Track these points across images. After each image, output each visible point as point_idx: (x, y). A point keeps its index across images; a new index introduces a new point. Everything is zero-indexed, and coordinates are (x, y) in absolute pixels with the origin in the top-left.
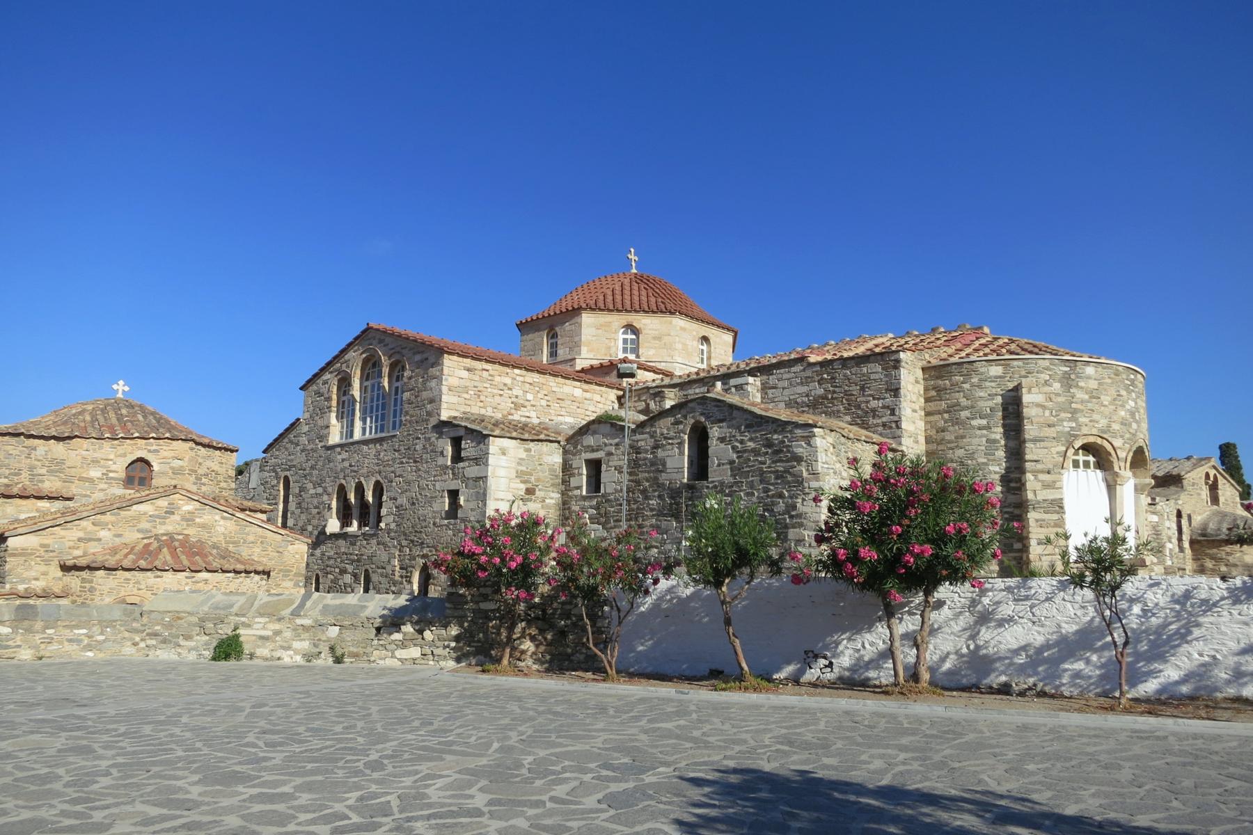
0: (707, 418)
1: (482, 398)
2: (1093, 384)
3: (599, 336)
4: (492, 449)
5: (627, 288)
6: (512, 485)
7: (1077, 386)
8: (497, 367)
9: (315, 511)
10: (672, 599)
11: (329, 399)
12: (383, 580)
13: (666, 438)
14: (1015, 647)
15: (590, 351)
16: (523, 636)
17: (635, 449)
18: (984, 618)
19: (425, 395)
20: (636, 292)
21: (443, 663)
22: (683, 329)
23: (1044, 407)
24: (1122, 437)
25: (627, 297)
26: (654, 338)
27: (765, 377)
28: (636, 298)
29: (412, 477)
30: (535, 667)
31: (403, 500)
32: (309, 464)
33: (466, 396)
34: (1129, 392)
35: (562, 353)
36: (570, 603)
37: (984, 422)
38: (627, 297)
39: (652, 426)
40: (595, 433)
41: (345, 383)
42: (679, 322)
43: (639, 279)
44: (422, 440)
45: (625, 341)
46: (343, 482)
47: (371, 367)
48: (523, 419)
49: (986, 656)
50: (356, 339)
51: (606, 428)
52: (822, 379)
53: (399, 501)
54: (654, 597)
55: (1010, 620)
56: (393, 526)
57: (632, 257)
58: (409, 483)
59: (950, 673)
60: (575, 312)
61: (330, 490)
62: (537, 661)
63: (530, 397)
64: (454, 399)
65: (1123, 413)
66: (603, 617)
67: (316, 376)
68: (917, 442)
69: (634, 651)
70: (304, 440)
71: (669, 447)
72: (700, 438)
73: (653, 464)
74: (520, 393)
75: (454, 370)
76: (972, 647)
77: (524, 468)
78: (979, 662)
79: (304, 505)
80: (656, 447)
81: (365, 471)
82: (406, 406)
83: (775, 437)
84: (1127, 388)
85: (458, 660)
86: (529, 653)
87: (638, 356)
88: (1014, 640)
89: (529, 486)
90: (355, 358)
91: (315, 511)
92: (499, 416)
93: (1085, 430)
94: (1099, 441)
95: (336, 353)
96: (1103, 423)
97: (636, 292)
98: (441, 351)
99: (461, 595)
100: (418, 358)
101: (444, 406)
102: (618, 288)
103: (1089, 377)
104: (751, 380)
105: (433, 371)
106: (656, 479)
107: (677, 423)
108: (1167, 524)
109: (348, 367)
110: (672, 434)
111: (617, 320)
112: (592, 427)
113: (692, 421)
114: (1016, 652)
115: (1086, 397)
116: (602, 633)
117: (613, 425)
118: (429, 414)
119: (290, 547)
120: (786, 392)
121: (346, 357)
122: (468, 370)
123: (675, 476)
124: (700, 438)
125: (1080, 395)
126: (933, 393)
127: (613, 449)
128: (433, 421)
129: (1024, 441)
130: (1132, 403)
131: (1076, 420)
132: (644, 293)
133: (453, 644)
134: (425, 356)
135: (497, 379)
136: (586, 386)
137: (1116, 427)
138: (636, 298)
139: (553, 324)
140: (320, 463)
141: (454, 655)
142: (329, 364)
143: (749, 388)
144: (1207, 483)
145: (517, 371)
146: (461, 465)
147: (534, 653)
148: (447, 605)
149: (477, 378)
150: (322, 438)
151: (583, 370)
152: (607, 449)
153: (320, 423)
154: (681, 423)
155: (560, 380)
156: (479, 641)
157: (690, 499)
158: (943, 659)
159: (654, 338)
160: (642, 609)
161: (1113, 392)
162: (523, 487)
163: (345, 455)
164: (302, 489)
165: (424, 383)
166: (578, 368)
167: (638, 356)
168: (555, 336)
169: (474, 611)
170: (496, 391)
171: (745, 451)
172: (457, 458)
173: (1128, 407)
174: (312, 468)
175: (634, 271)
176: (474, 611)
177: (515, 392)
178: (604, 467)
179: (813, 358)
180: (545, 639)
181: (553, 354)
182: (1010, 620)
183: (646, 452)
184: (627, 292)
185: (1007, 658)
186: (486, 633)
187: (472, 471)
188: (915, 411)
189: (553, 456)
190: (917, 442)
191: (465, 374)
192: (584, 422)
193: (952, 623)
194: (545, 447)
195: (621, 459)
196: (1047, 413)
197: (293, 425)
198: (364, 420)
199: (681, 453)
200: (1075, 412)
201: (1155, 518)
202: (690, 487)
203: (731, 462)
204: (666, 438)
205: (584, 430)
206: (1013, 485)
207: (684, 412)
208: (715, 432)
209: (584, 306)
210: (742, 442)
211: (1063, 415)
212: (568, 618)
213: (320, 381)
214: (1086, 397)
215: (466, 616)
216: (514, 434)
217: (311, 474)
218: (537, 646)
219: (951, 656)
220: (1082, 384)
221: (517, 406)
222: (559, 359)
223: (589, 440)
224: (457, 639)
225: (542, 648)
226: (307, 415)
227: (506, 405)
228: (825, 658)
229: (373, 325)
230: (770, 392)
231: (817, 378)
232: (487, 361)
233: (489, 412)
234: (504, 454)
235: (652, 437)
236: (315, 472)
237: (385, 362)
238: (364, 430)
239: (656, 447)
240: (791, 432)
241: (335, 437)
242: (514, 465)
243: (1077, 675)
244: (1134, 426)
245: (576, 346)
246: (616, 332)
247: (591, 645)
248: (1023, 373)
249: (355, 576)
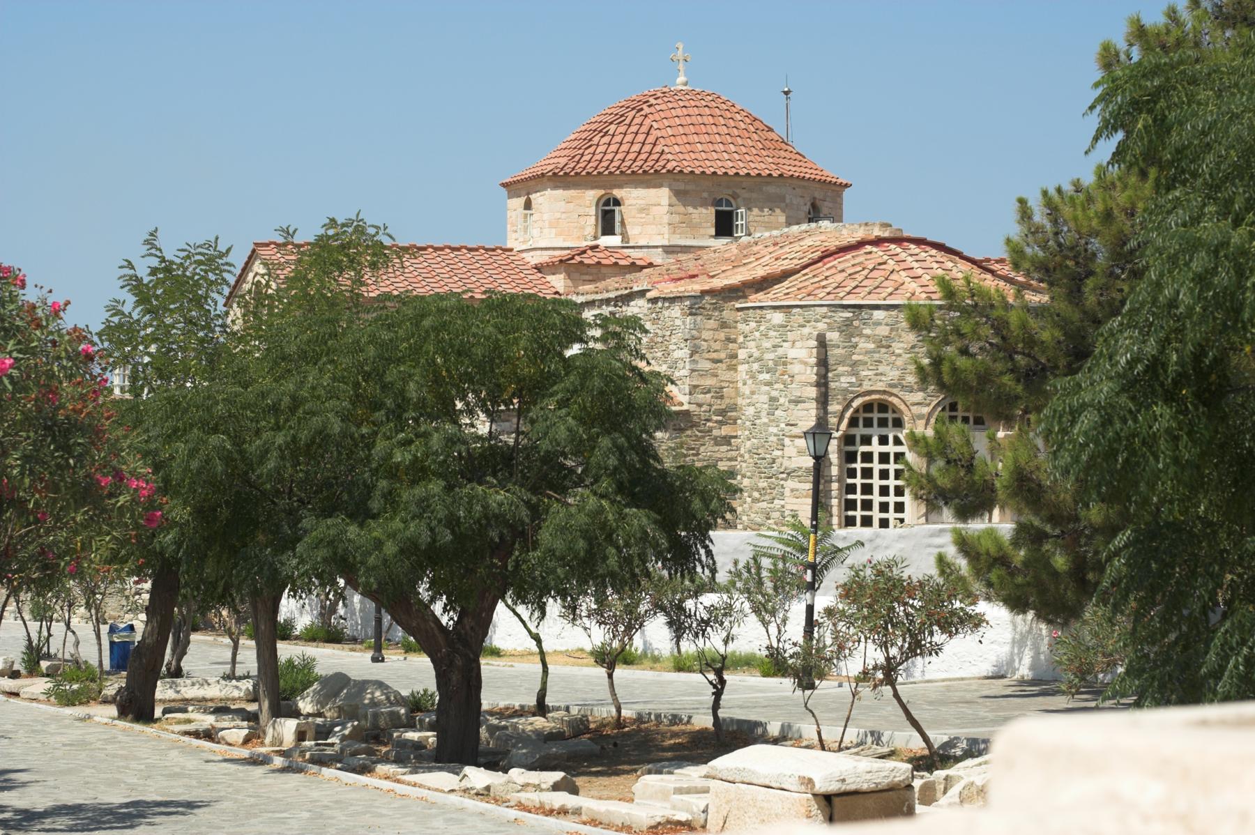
2: (883, 331)
7: (861, 335)
23: (806, 364)
93: (866, 386)
96: (893, 374)
103: (878, 324)
115: (873, 346)
125: (864, 345)
131: (856, 374)
200: (855, 364)
220: (867, 331)
248: (801, 320)
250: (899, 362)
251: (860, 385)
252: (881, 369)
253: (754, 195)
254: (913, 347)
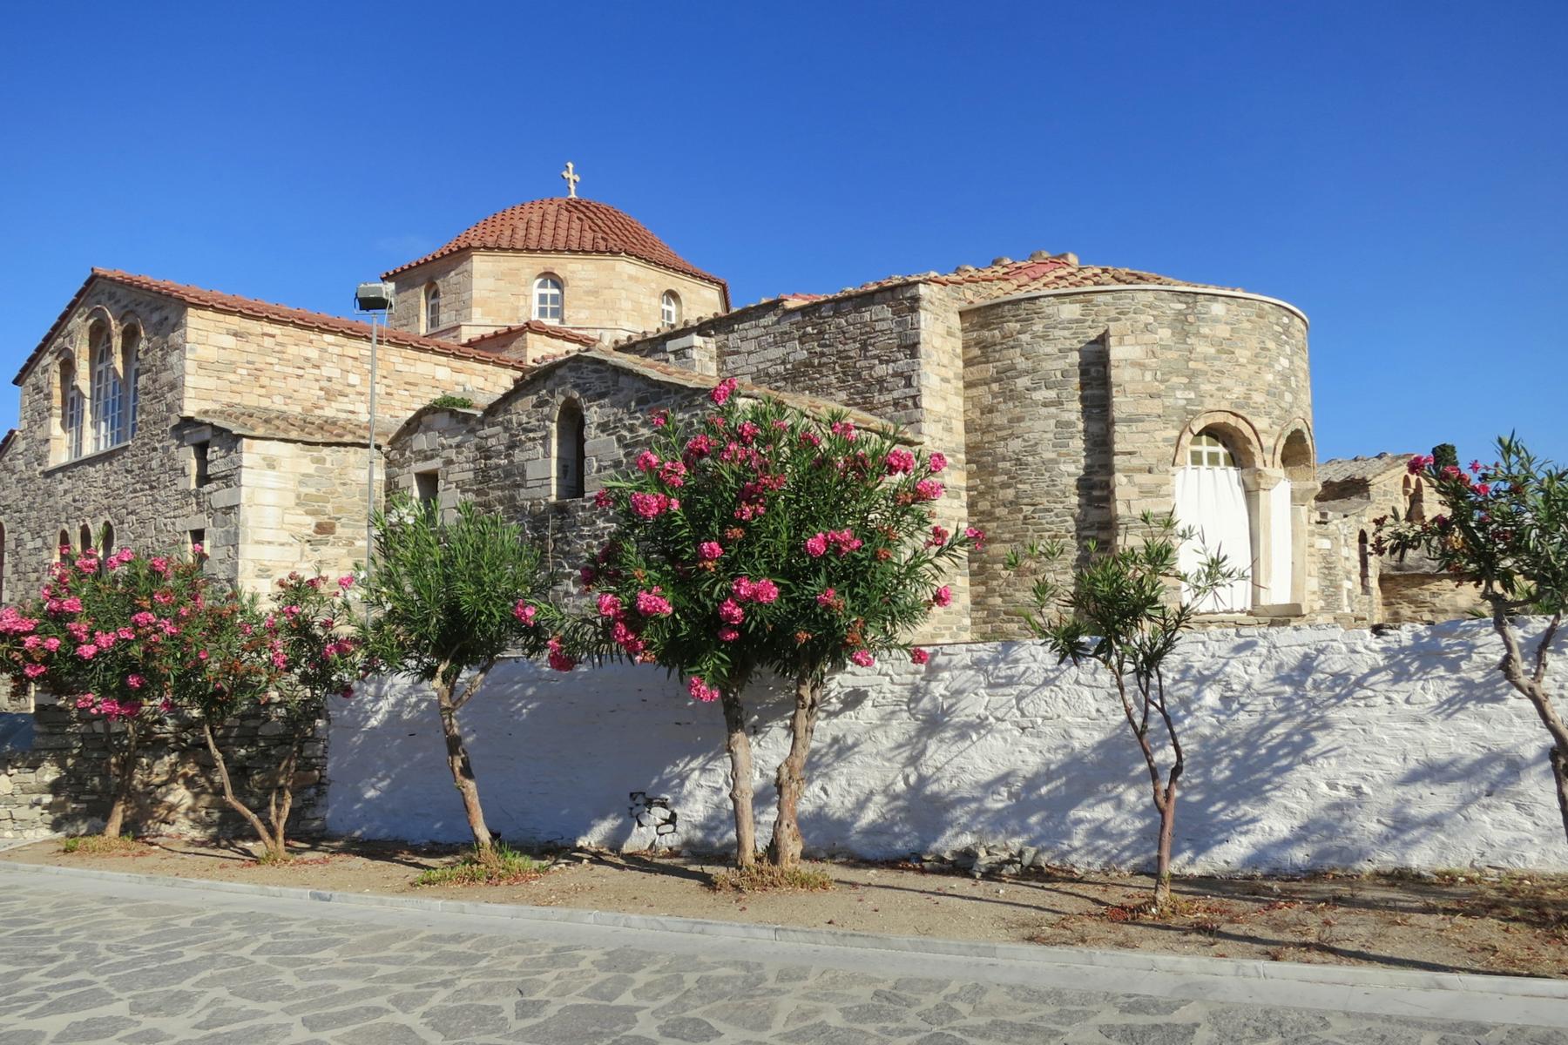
0: (583, 392)
1: (264, 381)
2: (1223, 331)
3: (497, 290)
4: (247, 459)
5: (551, 218)
6: (288, 518)
7: (1197, 334)
8: (290, 330)
9: (33, 576)
10: (420, 701)
11: (48, 397)
13: (526, 430)
14: (989, 777)
15: (485, 314)
16: (172, 778)
17: (486, 453)
18: (934, 723)
19: (165, 377)
20: (563, 225)
21: (30, 835)
22: (631, 277)
23: (1142, 366)
24: (1268, 414)
25: (548, 231)
26: (588, 293)
27: (722, 337)
28: (562, 233)
29: (146, 512)
30: (197, 834)
32: (25, 503)
33: (232, 377)
34: (1280, 344)
35: (446, 319)
36: (256, 716)
37: (1052, 394)
38: (548, 231)
39: (506, 411)
40: (428, 429)
41: (68, 368)
42: (626, 268)
43: (572, 206)
44: (160, 454)
45: (543, 298)
46: (66, 527)
47: (99, 335)
48: (344, 415)
49: (936, 797)
50: (80, 295)
51: (442, 420)
52: (805, 334)
54: (392, 700)
55: (980, 725)
57: (570, 175)
58: (142, 522)
59: (874, 830)
60: (460, 255)
61: (50, 540)
62: (199, 823)
63: (353, 379)
64: (210, 383)
65: (1270, 377)
66: (315, 739)
67: (33, 360)
68: (950, 430)
69: (358, 798)
70: (20, 464)
71: (529, 444)
72: (573, 422)
73: (508, 474)
74: (336, 373)
75: (205, 336)
76: (912, 779)
77: (312, 491)
78: (925, 808)
79: (22, 568)
80: (512, 446)
81: (90, 508)
82: (141, 398)
83: (680, 416)
84: (1276, 337)
85: (56, 826)
86: (182, 809)
87: (562, 321)
88: (987, 766)
89: (324, 519)
90: (80, 325)
91: (33, 576)
92: (295, 410)
93: (1210, 404)
94: (1232, 421)
95: (55, 320)
96: (1238, 391)
97: (563, 225)
98: (183, 304)
99: (61, 709)
100: (156, 317)
101: (189, 393)
102: (536, 218)
103: (1216, 320)
104: (697, 340)
105: (175, 337)
106: (512, 498)
107: (541, 404)
108: (1345, 552)
109: (71, 342)
110: (534, 422)
111: (530, 266)
112: (425, 419)
113: (561, 399)
114: (990, 787)
115: (1212, 351)
116: (313, 767)
117: (453, 413)
118: (170, 409)
120: (753, 359)
121: (70, 326)
122: (235, 335)
123: (539, 493)
124: (573, 422)
125: (1203, 348)
126: (976, 352)
127: (452, 453)
128: (175, 420)
129: (1113, 423)
130: (1285, 362)
131: (1195, 388)
132: (576, 224)
133: (48, 799)
134: (164, 313)
135: (292, 350)
136: (458, 364)
137: (1258, 398)
138: (562, 233)
139: (430, 275)
140: (39, 500)
141: (49, 818)
142: (48, 339)
143: (695, 354)
144: (1406, 493)
145: (328, 338)
146: (207, 488)
147: (192, 809)
148: (36, 728)
149: (253, 348)
150: (41, 459)
151: (470, 344)
152: (445, 453)
153: (39, 435)
154: (546, 403)
155: (410, 352)
156: (93, 791)
157: (560, 529)
158: (861, 805)
159: (588, 293)
160: (373, 722)
161: (1254, 343)
162: (311, 521)
163: (67, 484)
164: (19, 543)
165: (163, 358)
166: (464, 341)
167: (562, 321)
168: (436, 295)
169: (82, 737)
170: (290, 370)
171: (636, 444)
172: (204, 479)
173: (1278, 367)
174: (30, 508)
175: (573, 195)
176: (82, 737)
177: (325, 372)
178: (441, 484)
179: (792, 303)
180: (212, 782)
181: (434, 322)
182: (980, 725)
183: (498, 456)
184: (549, 224)
185: (974, 799)
186: (105, 776)
187: (221, 497)
188: (945, 380)
189: (363, 472)
190: (950, 430)
191: (230, 341)
192: (411, 414)
193: (879, 734)
194: (353, 455)
195: (463, 471)
196: (1148, 376)
197: (6, 440)
198: (95, 425)
199: (547, 454)
200: (1193, 375)
201: (1326, 544)
202: (560, 510)
203: (617, 464)
204: (526, 430)
205: (414, 425)
206: (1096, 493)
207: (550, 384)
208: (593, 415)
209: (476, 244)
210: (631, 429)
211: (1175, 380)
212: (253, 743)
213: (38, 369)
214: (1212, 351)
215: (70, 748)
216: (294, 435)
217: (28, 518)
218: (196, 796)
219: (878, 798)
220: (1205, 330)
221: (330, 395)
222: (442, 327)
223: (421, 441)
224: (54, 788)
225: (205, 800)
226: (24, 425)
227: (309, 392)
228: (664, 805)
229: (101, 270)
230: (729, 359)
231: (797, 334)
232: (272, 321)
233: (278, 404)
234: (271, 466)
235: (506, 429)
237: (116, 327)
238: (97, 440)
239: (512, 446)
240: (702, 406)
241: (60, 455)
242: (291, 485)
243: (1099, 831)
244: (1288, 397)
245: (464, 307)
246: (527, 284)
247: (229, 798)
248: (1113, 314)
250: (1244, 376)
251: (1202, 403)
252: (1227, 382)
253: (693, 296)
254: (1257, 356)
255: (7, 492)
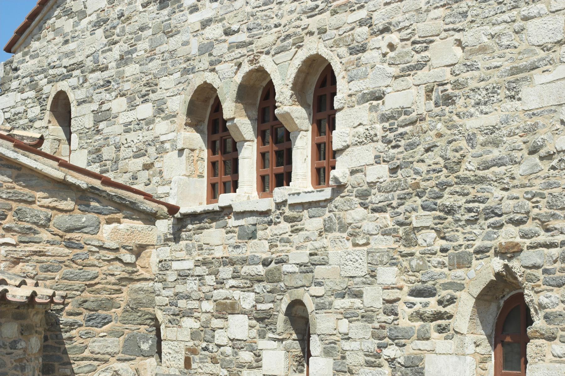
12: (358, 330)
31: (405, 96)
32: (117, 51)
53: (392, 102)
56: (381, 172)
119: (106, 230)
140: (143, 46)
174: (123, 60)
217: (121, 75)
236: (131, 70)
249: (263, 319)
255: (72, 46)
